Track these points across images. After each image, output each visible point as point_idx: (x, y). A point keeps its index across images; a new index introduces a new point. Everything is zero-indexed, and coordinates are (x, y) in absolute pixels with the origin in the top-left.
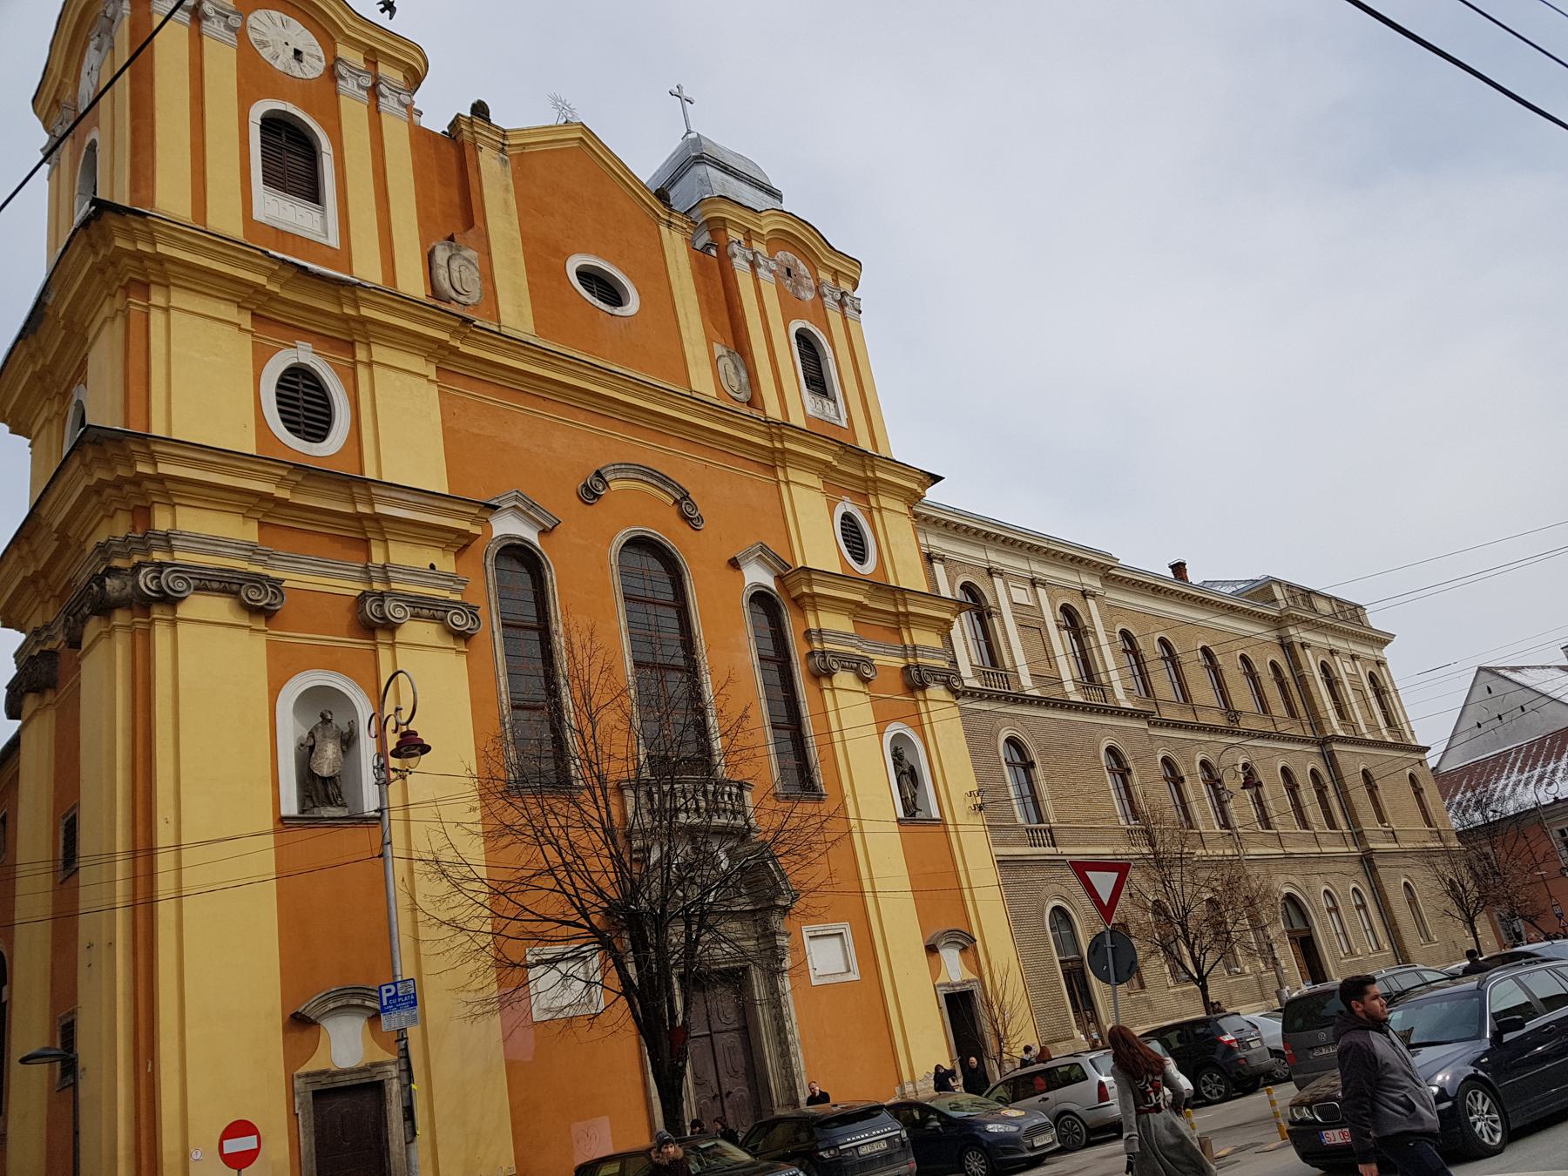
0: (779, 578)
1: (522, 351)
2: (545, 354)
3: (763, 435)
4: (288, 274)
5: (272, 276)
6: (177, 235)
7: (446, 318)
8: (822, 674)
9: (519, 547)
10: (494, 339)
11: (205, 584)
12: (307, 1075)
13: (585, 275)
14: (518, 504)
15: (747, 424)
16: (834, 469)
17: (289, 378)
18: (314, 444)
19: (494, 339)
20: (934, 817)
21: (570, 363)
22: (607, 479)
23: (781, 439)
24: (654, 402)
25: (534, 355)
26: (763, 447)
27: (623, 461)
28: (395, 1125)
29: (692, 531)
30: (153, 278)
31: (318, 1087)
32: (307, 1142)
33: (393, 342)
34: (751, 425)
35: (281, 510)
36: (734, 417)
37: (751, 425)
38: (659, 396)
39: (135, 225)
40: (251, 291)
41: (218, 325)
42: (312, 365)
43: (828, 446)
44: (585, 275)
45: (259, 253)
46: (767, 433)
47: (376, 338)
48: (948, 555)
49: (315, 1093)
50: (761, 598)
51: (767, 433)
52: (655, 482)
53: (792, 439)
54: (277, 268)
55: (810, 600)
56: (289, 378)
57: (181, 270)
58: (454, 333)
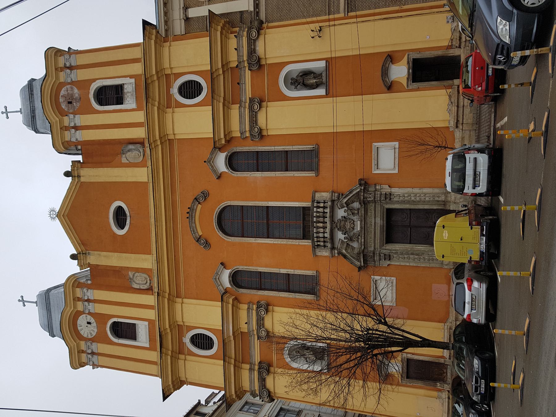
0: (221, 149)
1: (161, 270)
2: (159, 262)
3: (157, 151)
4: (164, 350)
5: (167, 354)
6: (165, 381)
7: (160, 302)
8: (261, 135)
9: (232, 278)
10: (160, 281)
11: (253, 50)
12: (402, 380)
13: (121, 226)
14: (217, 278)
15: (155, 162)
17: (195, 343)
18: (214, 342)
19: (160, 281)
20: (325, 65)
21: (159, 251)
22: (199, 237)
23: (155, 141)
24: (161, 211)
27: (190, 230)
28: (421, 358)
29: (209, 196)
30: (179, 381)
31: (405, 378)
32: (420, 384)
33: (174, 316)
34: (155, 159)
35: (227, 99)
36: (154, 170)
37: (155, 159)
38: (158, 209)
39: (166, 390)
40: (173, 358)
41: (186, 366)
42: (189, 338)
43: (150, 111)
44: (121, 226)
45: (161, 360)
46: (155, 148)
47: (174, 320)
48: (182, 6)
49: (407, 378)
50: (231, 162)
51: (155, 148)
52: (194, 214)
53: (154, 136)
54: (164, 354)
55: (227, 136)
56: (195, 343)
57: (174, 376)
58: (164, 297)
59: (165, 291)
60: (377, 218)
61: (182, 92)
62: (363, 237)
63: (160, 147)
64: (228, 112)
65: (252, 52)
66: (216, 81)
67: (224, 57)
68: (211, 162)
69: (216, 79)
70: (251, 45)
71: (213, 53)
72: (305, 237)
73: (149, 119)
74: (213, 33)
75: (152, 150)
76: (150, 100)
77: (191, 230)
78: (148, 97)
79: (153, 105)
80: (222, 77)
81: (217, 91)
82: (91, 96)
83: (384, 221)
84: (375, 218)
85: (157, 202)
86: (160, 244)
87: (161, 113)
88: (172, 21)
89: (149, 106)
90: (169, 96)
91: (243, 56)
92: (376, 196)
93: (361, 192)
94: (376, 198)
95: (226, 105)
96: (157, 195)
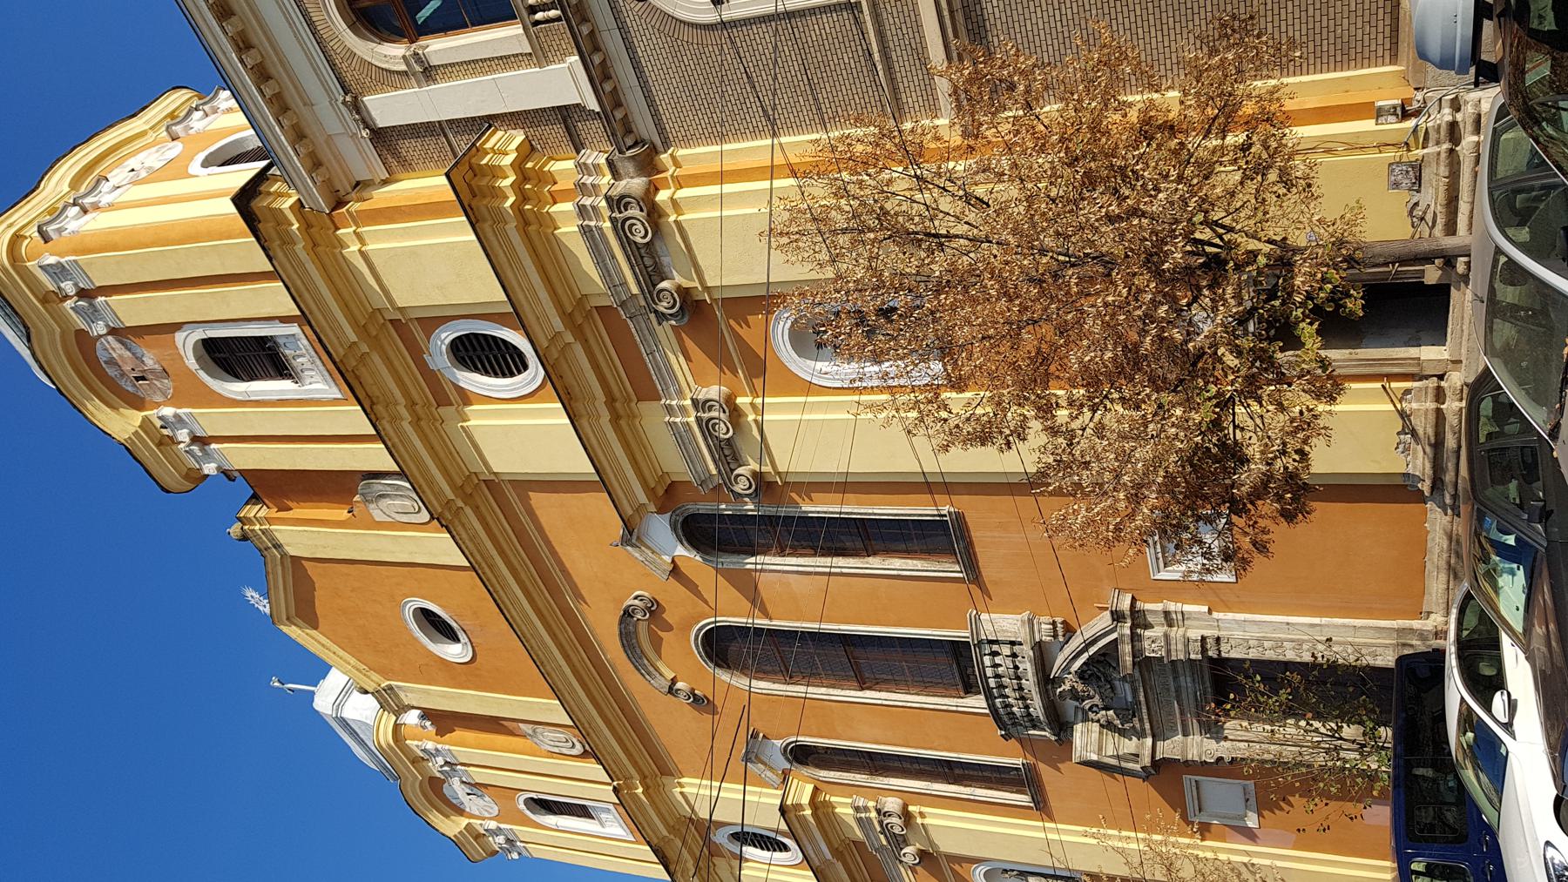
16: (411, 405)
25: (596, 739)
26: (476, 509)
53: (438, 494)
59: (629, 776)
60: (1182, 678)
61: (463, 358)
62: (1145, 717)
63: (468, 510)
64: (632, 428)
65: (650, 276)
66: (565, 366)
67: (560, 291)
68: (634, 541)
69: (562, 361)
70: (642, 257)
71: (521, 296)
72: (969, 688)
73: (404, 461)
74: (492, 238)
75: (450, 526)
76: (379, 408)
77: (642, 674)
78: (373, 403)
79: (395, 419)
80: (578, 349)
81: (577, 389)
82: (192, 363)
83: (1203, 683)
84: (1176, 678)
85: (523, 628)
86: (572, 703)
87: (428, 431)
88: (326, 142)
89: (384, 429)
90: (432, 379)
91: (624, 284)
92: (1173, 647)
93: (1123, 642)
94: (1173, 653)
95: (621, 412)
96: (514, 613)
